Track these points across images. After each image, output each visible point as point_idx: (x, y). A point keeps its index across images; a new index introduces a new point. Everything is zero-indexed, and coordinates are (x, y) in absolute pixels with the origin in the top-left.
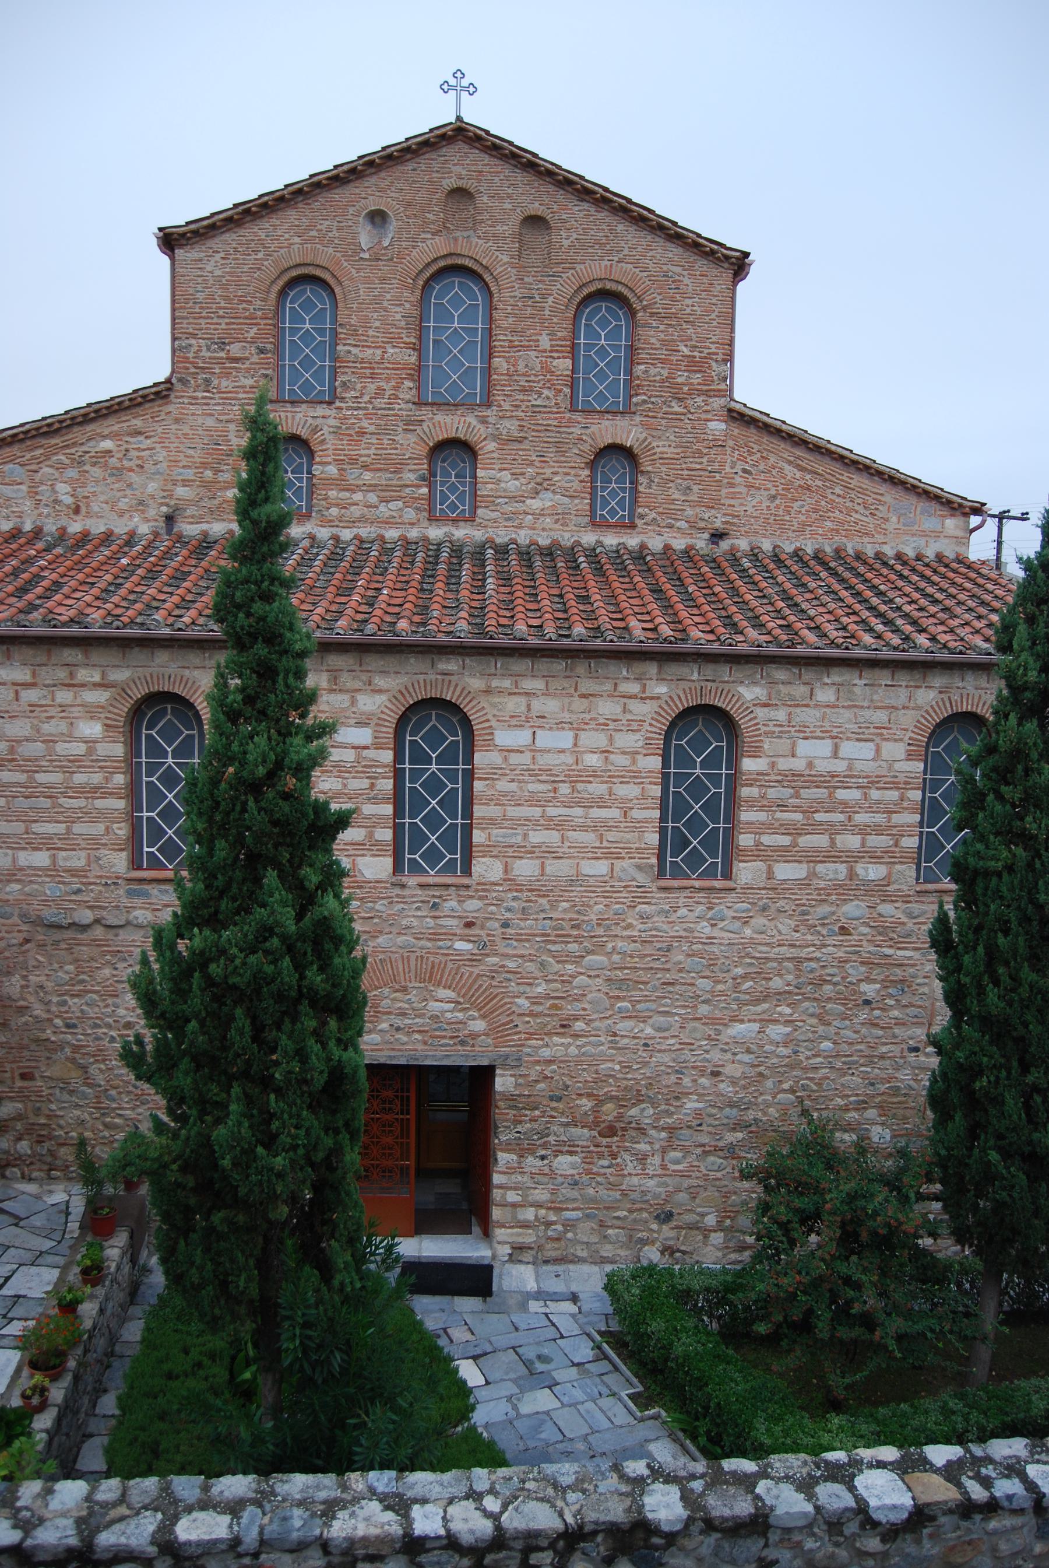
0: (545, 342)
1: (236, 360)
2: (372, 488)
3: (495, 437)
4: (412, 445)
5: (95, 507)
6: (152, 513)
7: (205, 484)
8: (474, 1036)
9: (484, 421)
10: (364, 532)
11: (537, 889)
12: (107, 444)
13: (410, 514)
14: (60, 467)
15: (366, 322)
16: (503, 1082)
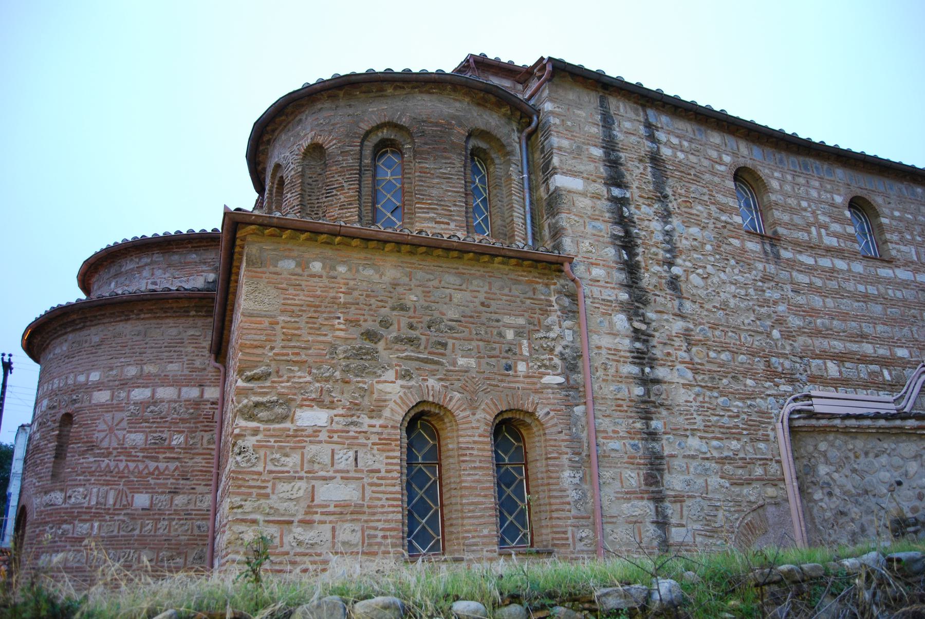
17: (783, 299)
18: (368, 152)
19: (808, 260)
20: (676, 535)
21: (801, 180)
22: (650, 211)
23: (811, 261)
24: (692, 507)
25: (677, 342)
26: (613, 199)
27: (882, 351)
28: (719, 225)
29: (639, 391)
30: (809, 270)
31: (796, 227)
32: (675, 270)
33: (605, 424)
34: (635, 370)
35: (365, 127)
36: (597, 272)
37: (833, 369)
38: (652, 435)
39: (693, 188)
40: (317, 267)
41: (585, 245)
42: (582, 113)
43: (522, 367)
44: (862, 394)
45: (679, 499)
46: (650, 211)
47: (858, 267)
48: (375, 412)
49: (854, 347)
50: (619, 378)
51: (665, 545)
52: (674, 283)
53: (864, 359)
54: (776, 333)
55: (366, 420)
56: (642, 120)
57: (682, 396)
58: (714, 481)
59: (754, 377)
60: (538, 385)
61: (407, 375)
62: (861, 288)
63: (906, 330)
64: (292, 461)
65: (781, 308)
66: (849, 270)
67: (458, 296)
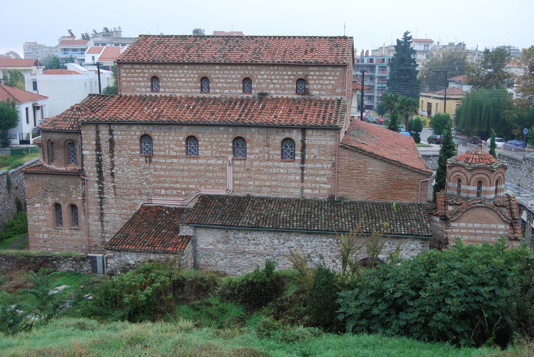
17: (150, 173)
18: (49, 144)
19: (162, 161)
20: (105, 228)
21: (167, 134)
22: (107, 156)
23: (164, 161)
24: (110, 224)
25: (111, 189)
26: (97, 155)
27: (184, 186)
28: (130, 156)
29: (100, 200)
30: (162, 164)
31: (160, 151)
32: (113, 171)
33: (91, 207)
34: (99, 196)
35: (48, 139)
36: (91, 174)
37: (163, 192)
38: (102, 209)
39: (123, 146)
40: (36, 178)
41: (89, 168)
42: (90, 132)
43: (73, 196)
44: (172, 198)
45: (107, 222)
46: (107, 156)
47: (182, 161)
48: (48, 204)
49: (173, 185)
50: (94, 197)
51: (103, 230)
52: (112, 175)
53: (176, 189)
54: (145, 183)
55: (46, 206)
56: (108, 129)
57: (111, 201)
58: (117, 218)
59: (134, 195)
60: (77, 199)
61: (52, 198)
62: (181, 168)
63: (196, 180)
64: (35, 212)
65: (149, 176)
66: (178, 162)
67: (61, 182)
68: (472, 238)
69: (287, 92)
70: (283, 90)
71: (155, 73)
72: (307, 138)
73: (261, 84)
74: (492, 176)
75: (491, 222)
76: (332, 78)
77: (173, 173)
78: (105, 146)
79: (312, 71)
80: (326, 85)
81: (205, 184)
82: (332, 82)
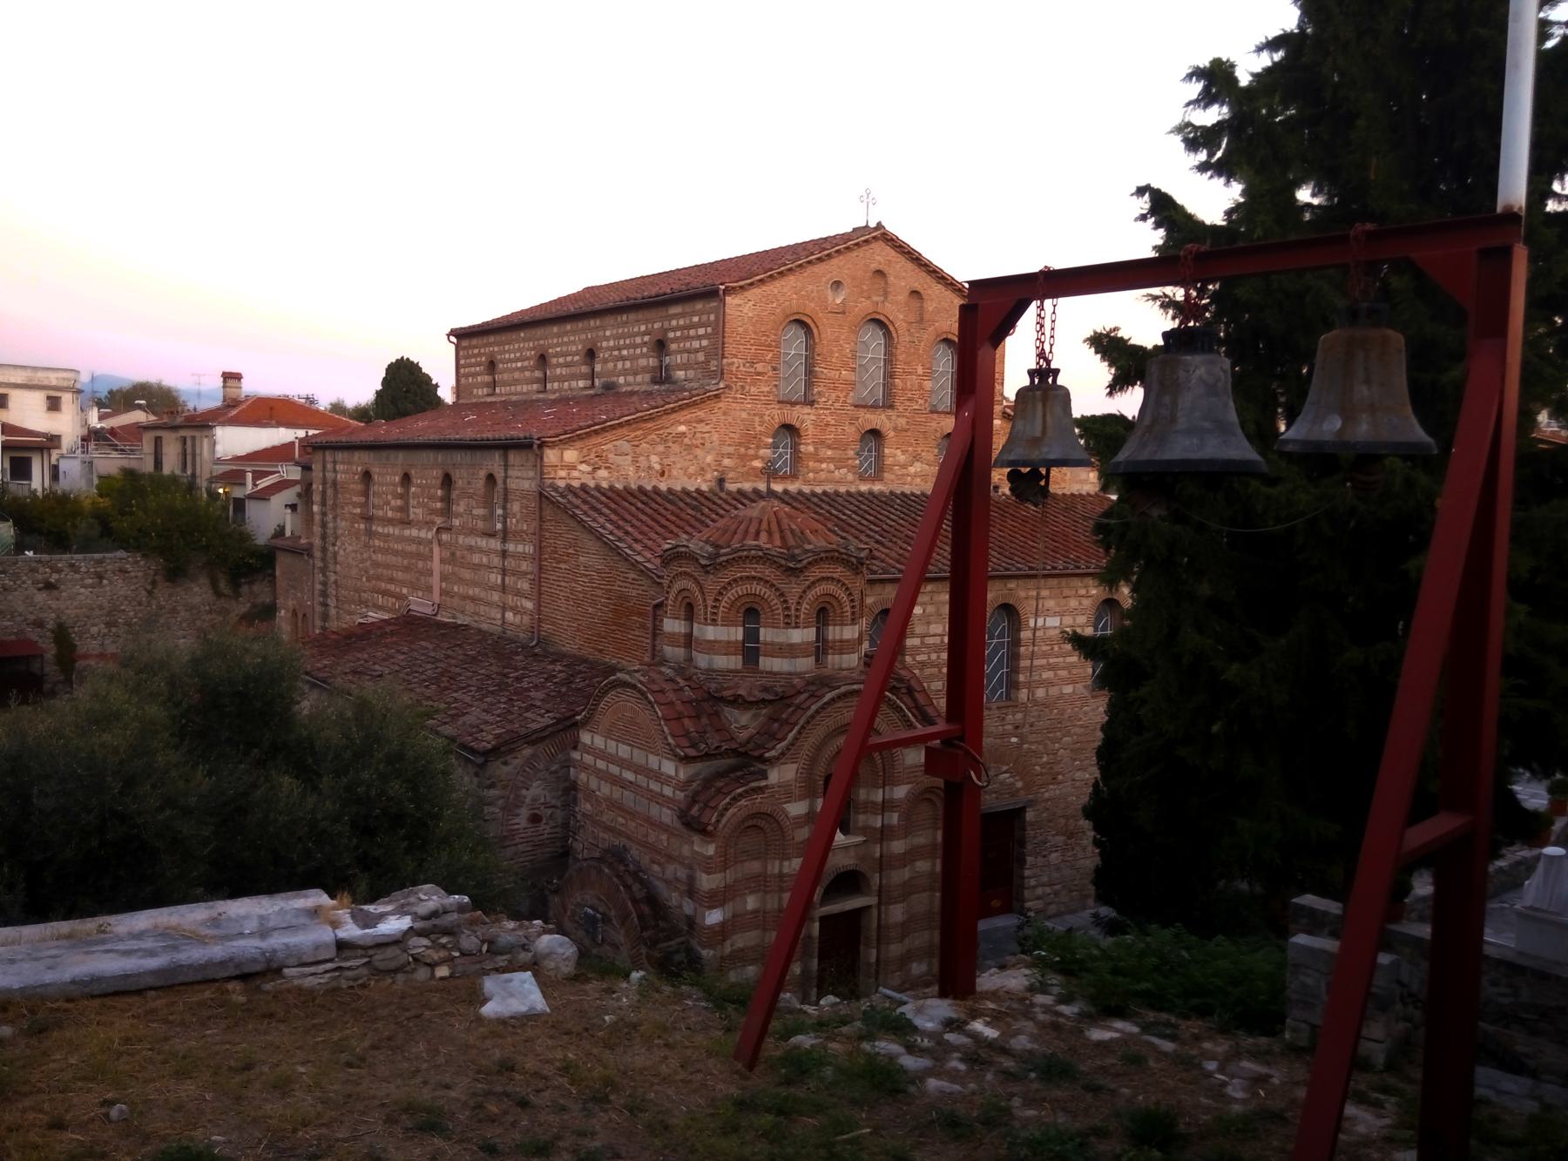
0: (920, 370)
1: (758, 374)
2: (831, 460)
3: (895, 429)
4: (851, 432)
5: (675, 473)
6: (708, 476)
7: (742, 458)
8: (1018, 790)
9: (889, 418)
10: (829, 488)
11: (1045, 705)
12: (682, 428)
13: (850, 477)
14: (653, 444)
15: (831, 352)
16: (1030, 815)
19: (380, 530)
68: (617, 793)
69: (639, 378)
70: (635, 374)
71: (492, 354)
72: (510, 473)
73: (605, 361)
74: (712, 583)
75: (648, 749)
76: (701, 331)
77: (391, 559)
78: (330, 492)
79: (675, 316)
80: (697, 351)
81: (414, 587)
82: (705, 343)
